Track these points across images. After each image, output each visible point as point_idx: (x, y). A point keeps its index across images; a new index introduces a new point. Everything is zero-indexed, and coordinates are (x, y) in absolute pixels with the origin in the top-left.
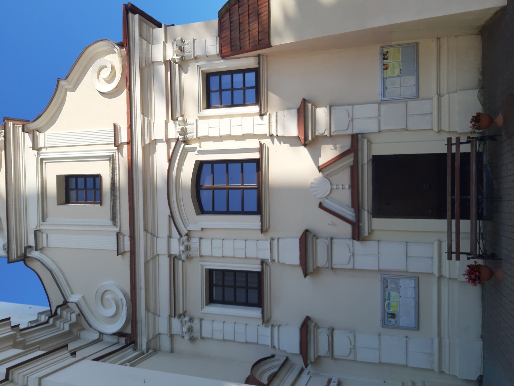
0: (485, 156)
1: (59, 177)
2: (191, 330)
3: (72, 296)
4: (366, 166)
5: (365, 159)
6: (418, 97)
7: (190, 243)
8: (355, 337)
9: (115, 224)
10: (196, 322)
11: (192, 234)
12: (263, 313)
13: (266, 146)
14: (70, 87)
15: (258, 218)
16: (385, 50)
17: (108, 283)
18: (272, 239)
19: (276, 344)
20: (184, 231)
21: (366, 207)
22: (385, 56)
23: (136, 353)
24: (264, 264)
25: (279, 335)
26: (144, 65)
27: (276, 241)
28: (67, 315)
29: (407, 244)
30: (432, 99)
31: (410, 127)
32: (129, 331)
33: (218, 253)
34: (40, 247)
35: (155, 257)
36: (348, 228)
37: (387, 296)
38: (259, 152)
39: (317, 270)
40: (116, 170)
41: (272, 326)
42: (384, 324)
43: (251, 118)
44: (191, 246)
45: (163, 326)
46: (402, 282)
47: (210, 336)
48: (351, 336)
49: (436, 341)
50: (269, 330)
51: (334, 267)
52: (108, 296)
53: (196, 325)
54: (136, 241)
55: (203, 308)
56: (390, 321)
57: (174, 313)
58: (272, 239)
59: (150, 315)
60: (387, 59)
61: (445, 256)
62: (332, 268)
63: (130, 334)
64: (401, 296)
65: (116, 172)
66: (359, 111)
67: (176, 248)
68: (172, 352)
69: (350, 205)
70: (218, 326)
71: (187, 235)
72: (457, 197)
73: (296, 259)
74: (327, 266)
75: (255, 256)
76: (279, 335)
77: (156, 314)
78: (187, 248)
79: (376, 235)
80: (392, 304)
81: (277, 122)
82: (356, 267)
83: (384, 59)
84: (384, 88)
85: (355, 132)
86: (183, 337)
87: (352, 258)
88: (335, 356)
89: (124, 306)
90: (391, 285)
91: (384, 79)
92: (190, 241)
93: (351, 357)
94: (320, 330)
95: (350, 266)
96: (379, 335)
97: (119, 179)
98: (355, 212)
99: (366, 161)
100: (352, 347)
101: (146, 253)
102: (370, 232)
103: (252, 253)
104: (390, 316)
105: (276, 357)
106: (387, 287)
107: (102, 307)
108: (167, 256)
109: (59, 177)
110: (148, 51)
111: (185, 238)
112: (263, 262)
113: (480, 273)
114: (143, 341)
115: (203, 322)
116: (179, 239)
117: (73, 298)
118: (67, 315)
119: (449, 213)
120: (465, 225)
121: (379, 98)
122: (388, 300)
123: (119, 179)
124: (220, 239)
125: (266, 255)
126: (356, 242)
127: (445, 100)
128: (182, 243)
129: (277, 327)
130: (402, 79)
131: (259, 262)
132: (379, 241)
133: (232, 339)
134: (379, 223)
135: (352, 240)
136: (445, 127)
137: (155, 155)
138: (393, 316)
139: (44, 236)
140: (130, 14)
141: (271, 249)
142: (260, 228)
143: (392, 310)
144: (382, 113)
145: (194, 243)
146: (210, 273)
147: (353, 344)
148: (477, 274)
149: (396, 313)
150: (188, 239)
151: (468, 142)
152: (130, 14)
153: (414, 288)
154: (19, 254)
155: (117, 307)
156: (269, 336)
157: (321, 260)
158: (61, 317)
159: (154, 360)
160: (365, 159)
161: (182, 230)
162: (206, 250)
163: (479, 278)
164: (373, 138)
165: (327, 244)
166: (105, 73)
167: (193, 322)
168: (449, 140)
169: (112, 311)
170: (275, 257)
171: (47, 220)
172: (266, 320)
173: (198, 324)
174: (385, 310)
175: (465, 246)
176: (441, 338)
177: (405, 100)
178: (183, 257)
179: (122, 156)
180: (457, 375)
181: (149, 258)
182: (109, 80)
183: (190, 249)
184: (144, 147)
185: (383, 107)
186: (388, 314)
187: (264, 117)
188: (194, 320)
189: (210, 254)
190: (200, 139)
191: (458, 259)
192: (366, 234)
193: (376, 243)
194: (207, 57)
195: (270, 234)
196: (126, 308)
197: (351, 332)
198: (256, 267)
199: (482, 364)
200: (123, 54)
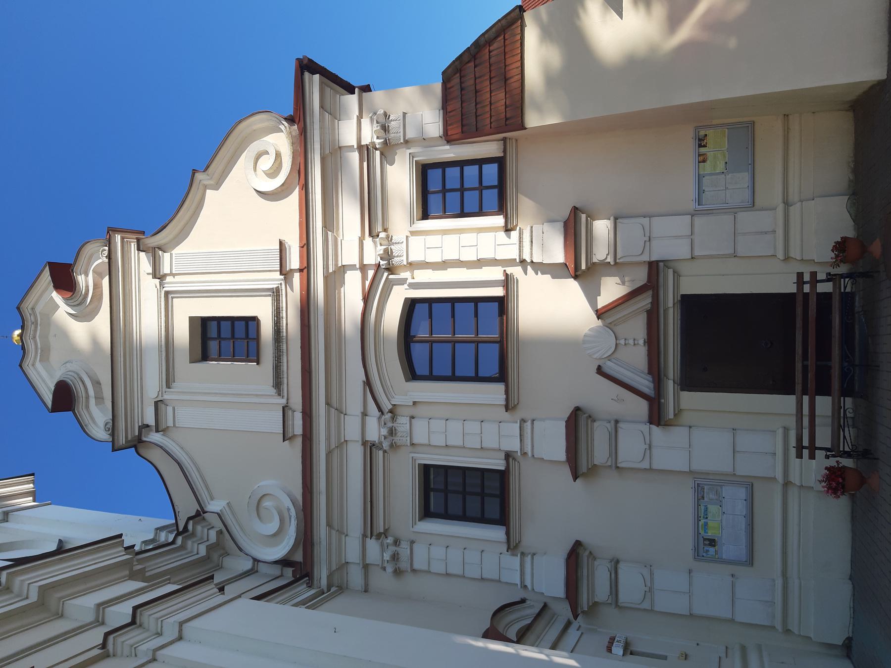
0: (857, 299)
1: (192, 319)
2: (396, 558)
3: (211, 502)
4: (671, 311)
5: (670, 300)
6: (754, 206)
7: (395, 425)
8: (652, 574)
9: (279, 393)
10: (405, 545)
11: (399, 411)
12: (508, 534)
13: (515, 277)
14: (212, 182)
15: (500, 387)
16: (702, 133)
17: (268, 484)
18: (523, 421)
19: (528, 583)
20: (387, 406)
21: (671, 375)
22: (701, 142)
23: (312, 592)
24: (511, 460)
25: (532, 569)
26: (327, 152)
27: (529, 424)
28: (203, 531)
29: (734, 432)
30: (775, 209)
31: (741, 252)
32: (299, 557)
33: (438, 440)
34: (162, 426)
35: (342, 444)
36: (641, 407)
37: (703, 511)
38: (504, 286)
39: (593, 470)
40: (282, 310)
41: (523, 554)
42: (698, 555)
43: (491, 235)
44: (396, 428)
45: (352, 552)
46: (727, 491)
47: (425, 567)
48: (646, 573)
49: (779, 583)
50: (517, 560)
51: (619, 465)
52: (267, 503)
53: (404, 550)
54: (314, 419)
55: (415, 524)
56: (707, 551)
57: (371, 530)
58: (523, 421)
59: (334, 532)
60: (705, 146)
61: (793, 452)
62: (617, 467)
63: (301, 562)
64: (724, 513)
65: (282, 313)
66: (660, 226)
67: (374, 432)
68: (366, 591)
69: (646, 371)
70: (438, 552)
71: (391, 411)
72: (811, 362)
73: (560, 453)
74: (609, 463)
75: (496, 446)
76: (532, 569)
77: (342, 533)
78: (392, 432)
79: (686, 418)
80: (710, 524)
81: (532, 242)
82: (655, 467)
83: (700, 146)
84: (700, 191)
85: (653, 259)
86: (384, 569)
87: (648, 452)
88: (621, 603)
89: (293, 519)
90: (709, 496)
91: (700, 178)
92: (395, 421)
93: (646, 605)
94: (596, 563)
95: (645, 465)
96: (690, 572)
97: (287, 324)
98: (654, 382)
99: (671, 304)
100: (647, 589)
101: (328, 438)
102: (676, 412)
103: (491, 441)
104: (707, 542)
105: (528, 602)
106: (703, 498)
107: (259, 521)
108: (360, 442)
109: (192, 319)
110: (334, 130)
111: (388, 416)
112: (508, 456)
113: (843, 479)
114: (322, 574)
115: (415, 546)
116: (379, 418)
117: (214, 506)
118: (203, 531)
119: (799, 388)
120: (824, 404)
121: (692, 206)
122: (704, 517)
123: (287, 324)
124: (441, 419)
125: (513, 445)
126: (654, 427)
127: (795, 210)
128: (383, 423)
129: (530, 556)
130: (729, 176)
131: (503, 456)
132: (690, 427)
133: (460, 572)
134: (692, 400)
135: (649, 424)
136: (795, 253)
137: (342, 289)
138: (712, 542)
139: (170, 410)
140: (307, 75)
141: (521, 435)
142: (504, 403)
143: (710, 534)
144: (696, 229)
145: (402, 423)
146: (426, 470)
147: (649, 584)
148: (841, 480)
149: (716, 539)
150: (393, 419)
151: (828, 280)
152: (307, 75)
153: (745, 500)
154: (130, 438)
155: (282, 521)
156: (517, 570)
157: (600, 453)
158: (193, 534)
159: (340, 601)
160: (670, 300)
161: (383, 403)
162: (420, 437)
163: (843, 487)
164: (684, 269)
165: (610, 430)
166: (266, 163)
167: (399, 545)
168: (800, 275)
169: (272, 527)
170: (528, 449)
171: (174, 385)
172: (512, 546)
173: (407, 549)
174: (699, 533)
175: (824, 438)
176: (787, 578)
177: (734, 211)
178: (386, 445)
179: (292, 290)
180: (812, 636)
181: (333, 446)
182: (272, 173)
183: (395, 434)
184: (326, 278)
185: (698, 220)
186: (705, 539)
187: (513, 233)
188: (402, 542)
189: (426, 442)
190: (412, 266)
191: (812, 457)
192: (671, 416)
193: (687, 429)
194: (425, 141)
195: (520, 414)
196: (296, 521)
197: (646, 566)
199: (852, 619)
200: (294, 134)
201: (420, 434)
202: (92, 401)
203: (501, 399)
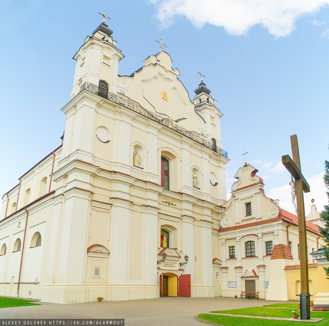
9: (242, 221)
20: (241, 240)
23: (217, 233)
53: (224, 245)
67: (238, 239)
79: (242, 280)
112: (237, 259)
114: (219, 233)
125: (238, 260)
134: (244, 281)
145: (239, 243)
201: (238, 246)
202: (238, 184)
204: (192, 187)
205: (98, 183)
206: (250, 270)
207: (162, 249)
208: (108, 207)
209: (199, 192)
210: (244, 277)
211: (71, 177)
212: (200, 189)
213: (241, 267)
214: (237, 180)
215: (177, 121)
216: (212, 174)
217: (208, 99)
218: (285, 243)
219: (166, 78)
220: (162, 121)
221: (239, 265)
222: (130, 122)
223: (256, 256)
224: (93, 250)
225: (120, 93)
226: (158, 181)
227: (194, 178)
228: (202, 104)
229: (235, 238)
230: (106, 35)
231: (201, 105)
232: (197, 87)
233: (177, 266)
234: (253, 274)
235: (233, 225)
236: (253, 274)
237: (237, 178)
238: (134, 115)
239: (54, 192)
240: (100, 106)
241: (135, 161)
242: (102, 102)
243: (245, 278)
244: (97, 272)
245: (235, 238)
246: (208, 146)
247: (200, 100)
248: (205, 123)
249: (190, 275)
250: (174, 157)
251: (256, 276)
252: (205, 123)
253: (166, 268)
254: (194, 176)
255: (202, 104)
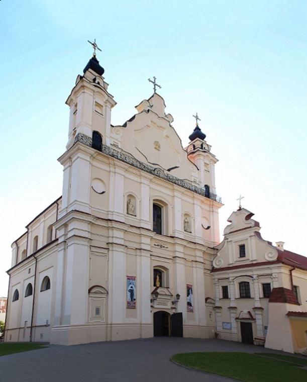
15: (239, 297)
67: (231, 279)
73: (231, 306)
103: (232, 296)
112: (230, 299)
145: (232, 283)
157: (232, 311)
162: (231, 286)
169: (217, 264)
198: (229, 297)
203: (237, 297)
204: (183, 231)
205: (96, 230)
206: (246, 311)
207: (155, 288)
208: (106, 251)
209: (191, 235)
210: (240, 318)
211: (70, 227)
212: (191, 232)
213: (235, 308)
214: (230, 223)
215: (169, 170)
216: (204, 219)
217: (202, 145)
218: (287, 286)
219: (158, 127)
220: (154, 170)
221: (232, 305)
222: (123, 173)
223: (252, 297)
224: (93, 291)
225: (114, 145)
226: (150, 227)
227: (185, 222)
228: (196, 150)
229: (227, 279)
230: (97, 74)
231: (195, 152)
232: (191, 132)
233: (169, 305)
234: (248, 316)
235: (226, 266)
236: (248, 316)
237: (230, 221)
238: (126, 166)
239: (57, 240)
240: (94, 158)
241: (129, 210)
242: (95, 155)
243: (240, 319)
244: (98, 311)
245: (227, 279)
246: (200, 192)
247: (194, 146)
248: (198, 170)
249: (182, 313)
250: (166, 204)
251: (252, 318)
252: (198, 170)
253: (159, 307)
254: (186, 221)
255: (196, 150)
